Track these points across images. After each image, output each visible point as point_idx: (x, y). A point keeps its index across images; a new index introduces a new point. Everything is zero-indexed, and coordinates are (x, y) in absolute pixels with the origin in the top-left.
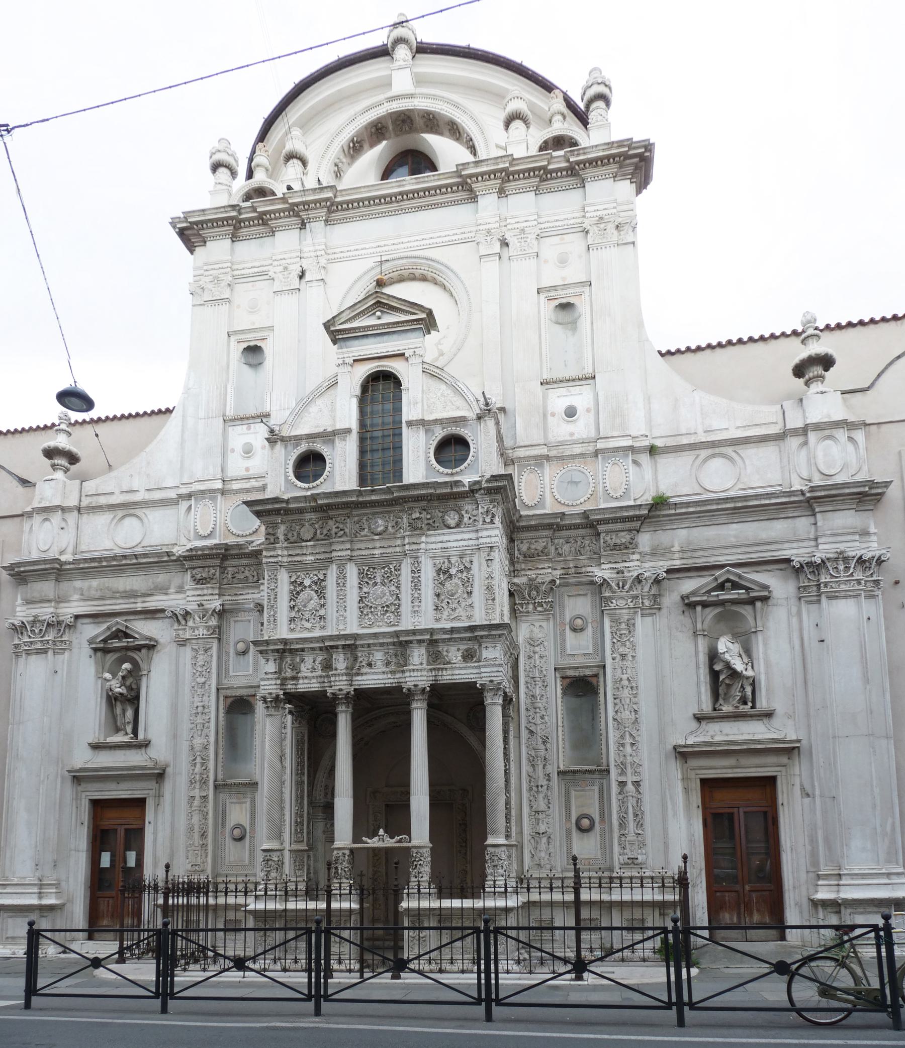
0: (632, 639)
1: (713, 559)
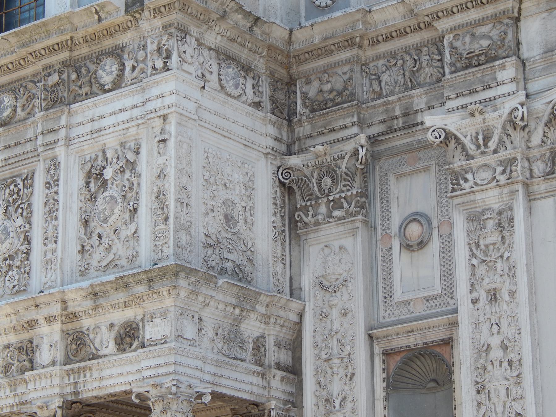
0: (506, 255)
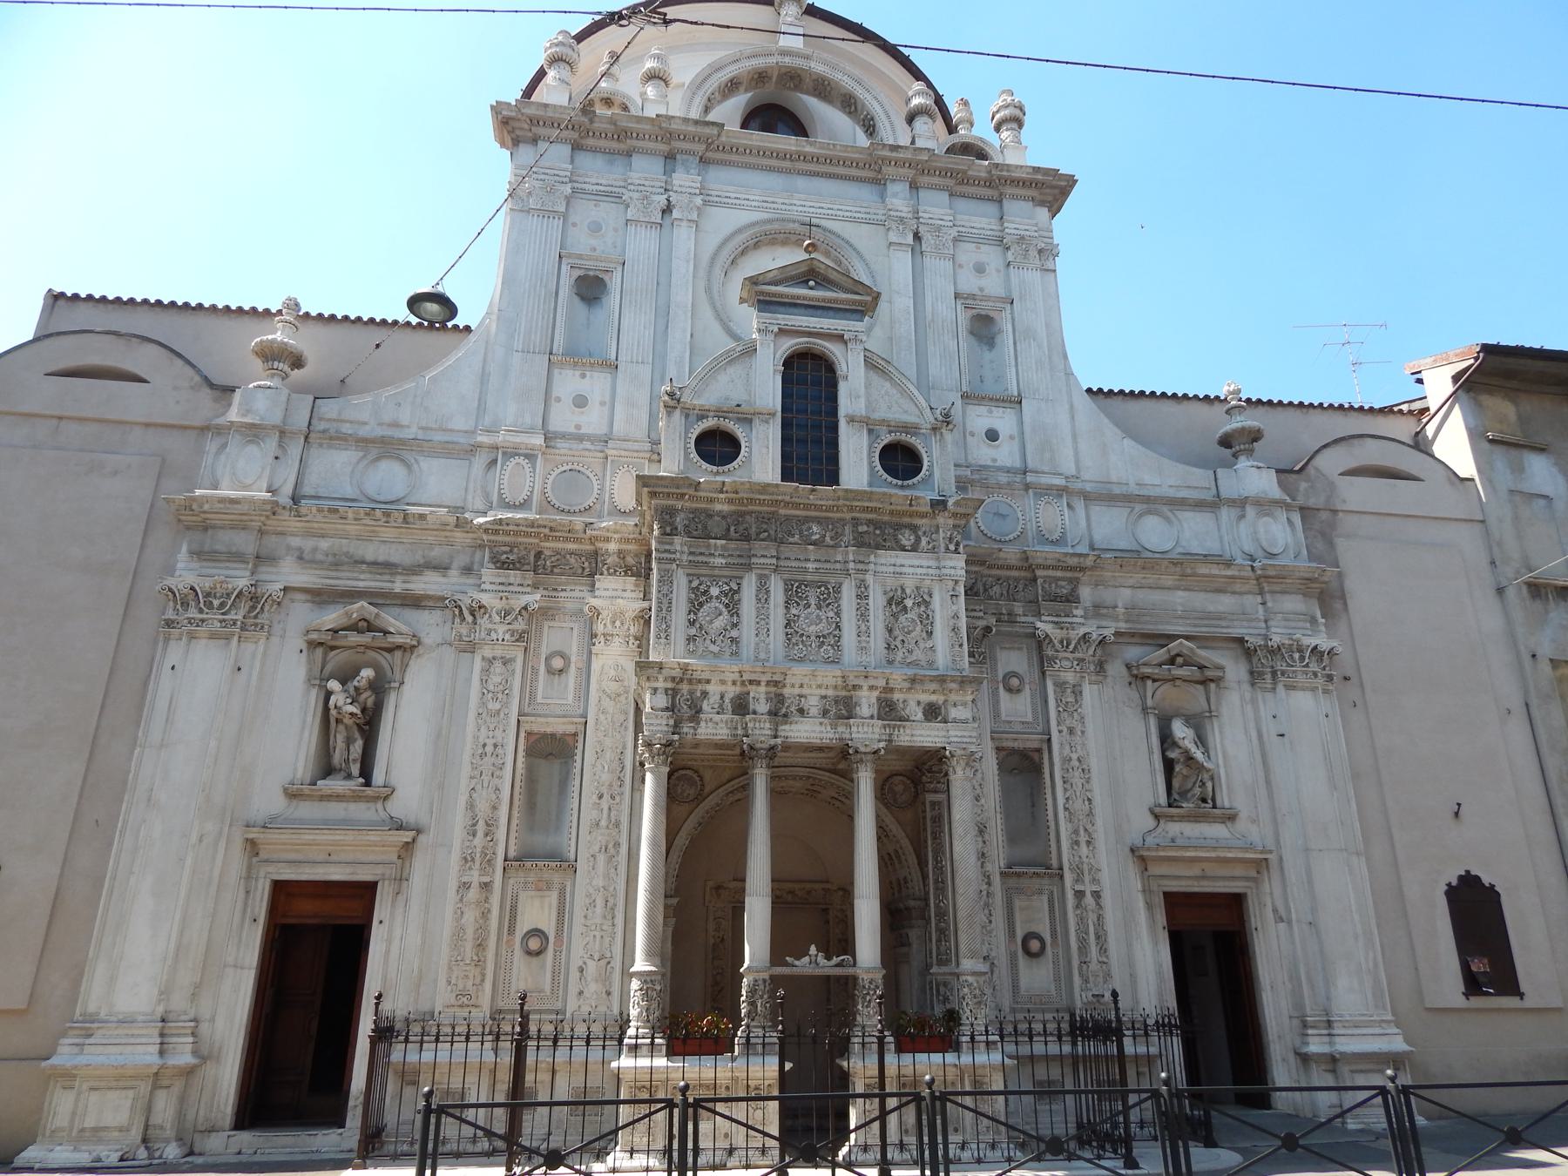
0: (1079, 710)
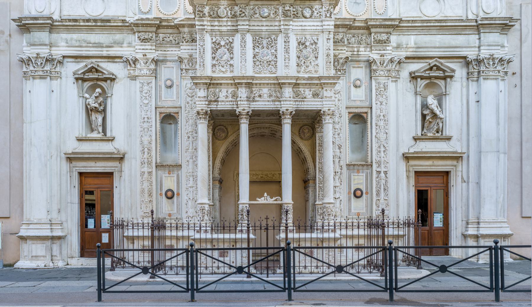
1: (427, 53)
